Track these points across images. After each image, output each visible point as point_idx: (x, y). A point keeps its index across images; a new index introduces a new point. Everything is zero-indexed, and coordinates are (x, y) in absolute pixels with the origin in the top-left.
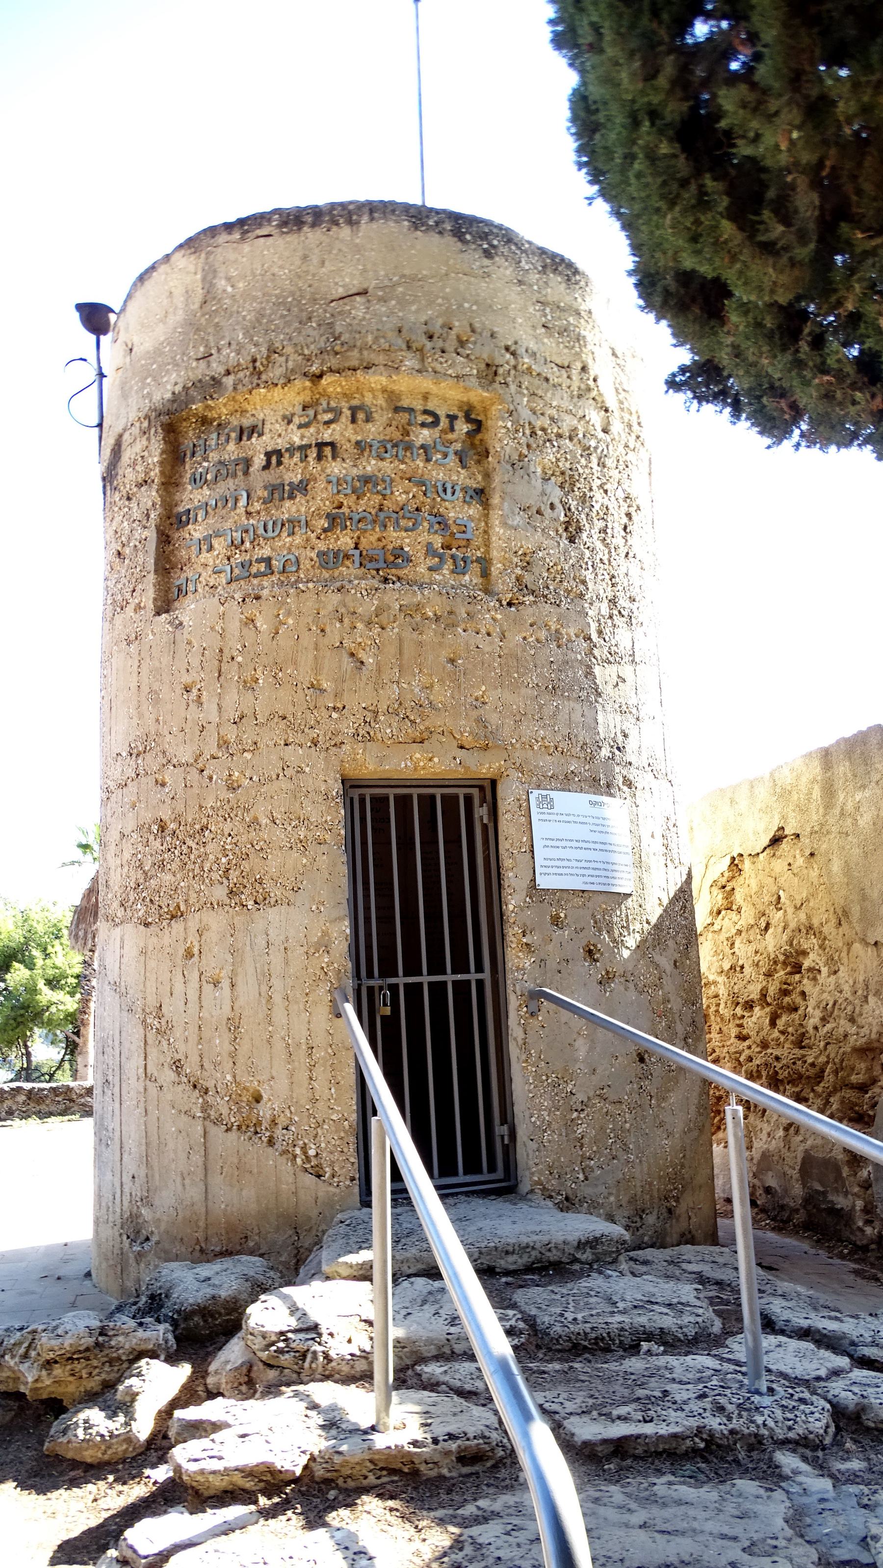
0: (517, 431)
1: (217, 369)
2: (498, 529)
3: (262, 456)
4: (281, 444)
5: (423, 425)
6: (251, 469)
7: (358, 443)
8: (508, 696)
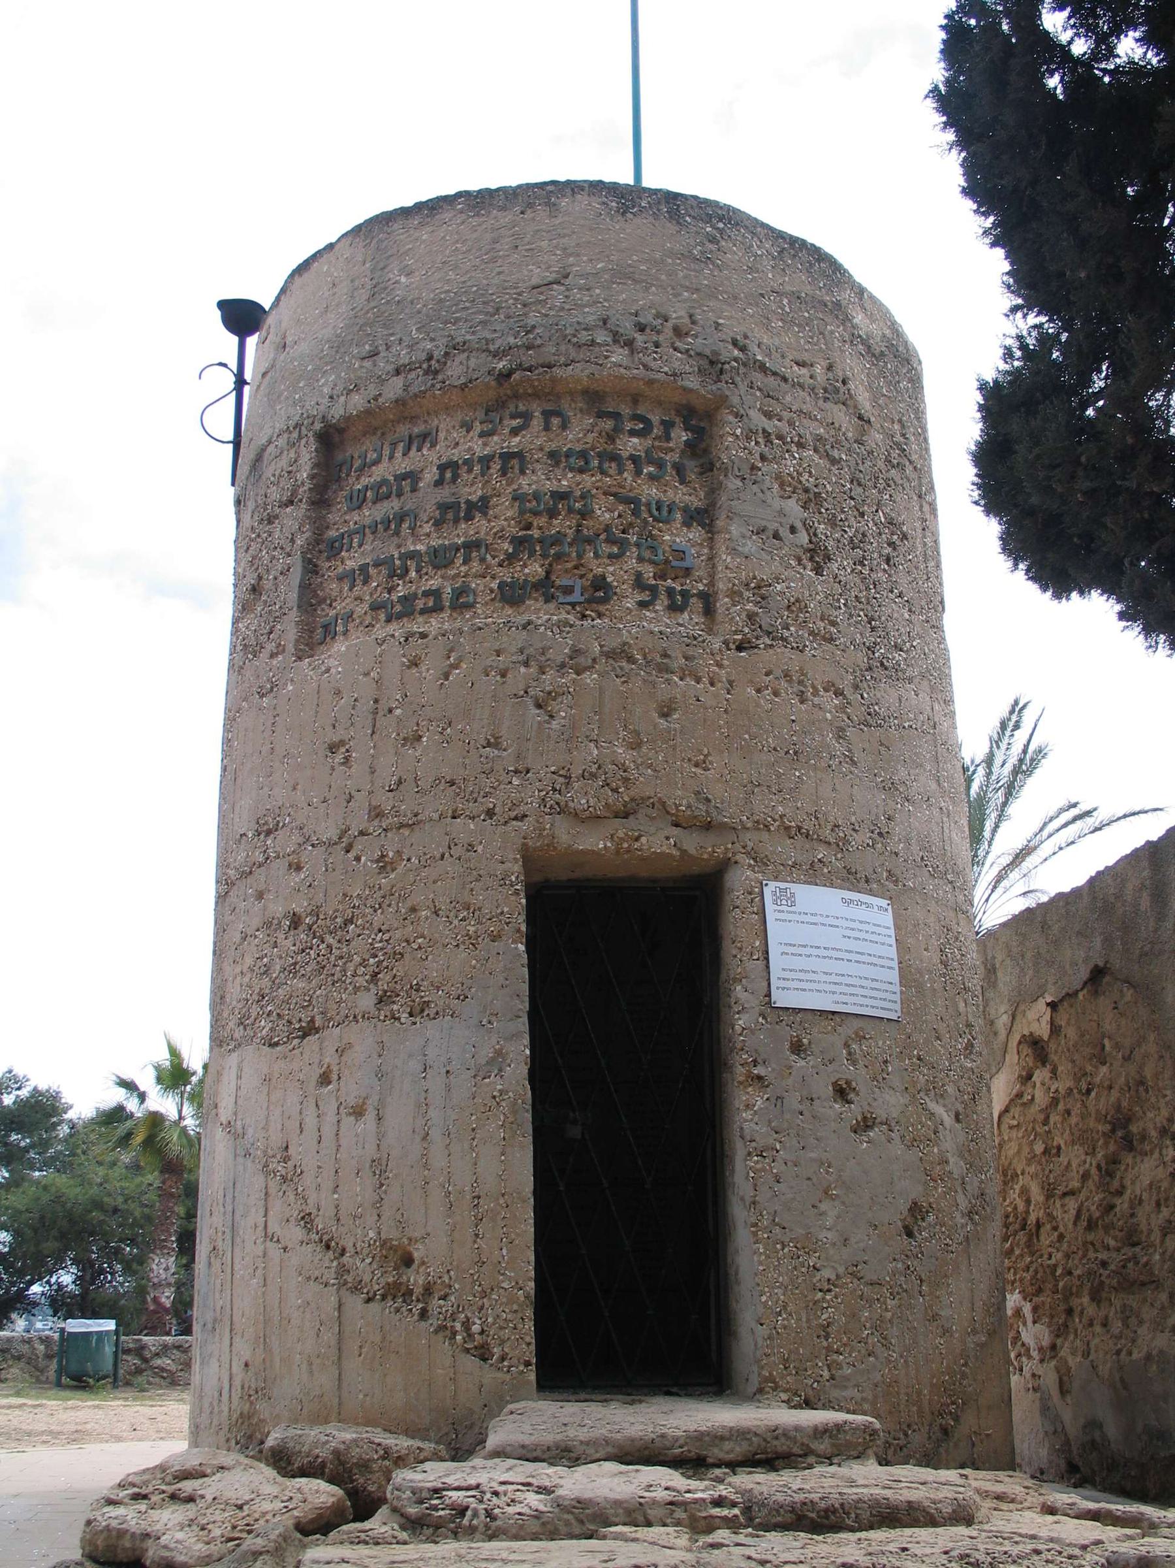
4: (456, 455)
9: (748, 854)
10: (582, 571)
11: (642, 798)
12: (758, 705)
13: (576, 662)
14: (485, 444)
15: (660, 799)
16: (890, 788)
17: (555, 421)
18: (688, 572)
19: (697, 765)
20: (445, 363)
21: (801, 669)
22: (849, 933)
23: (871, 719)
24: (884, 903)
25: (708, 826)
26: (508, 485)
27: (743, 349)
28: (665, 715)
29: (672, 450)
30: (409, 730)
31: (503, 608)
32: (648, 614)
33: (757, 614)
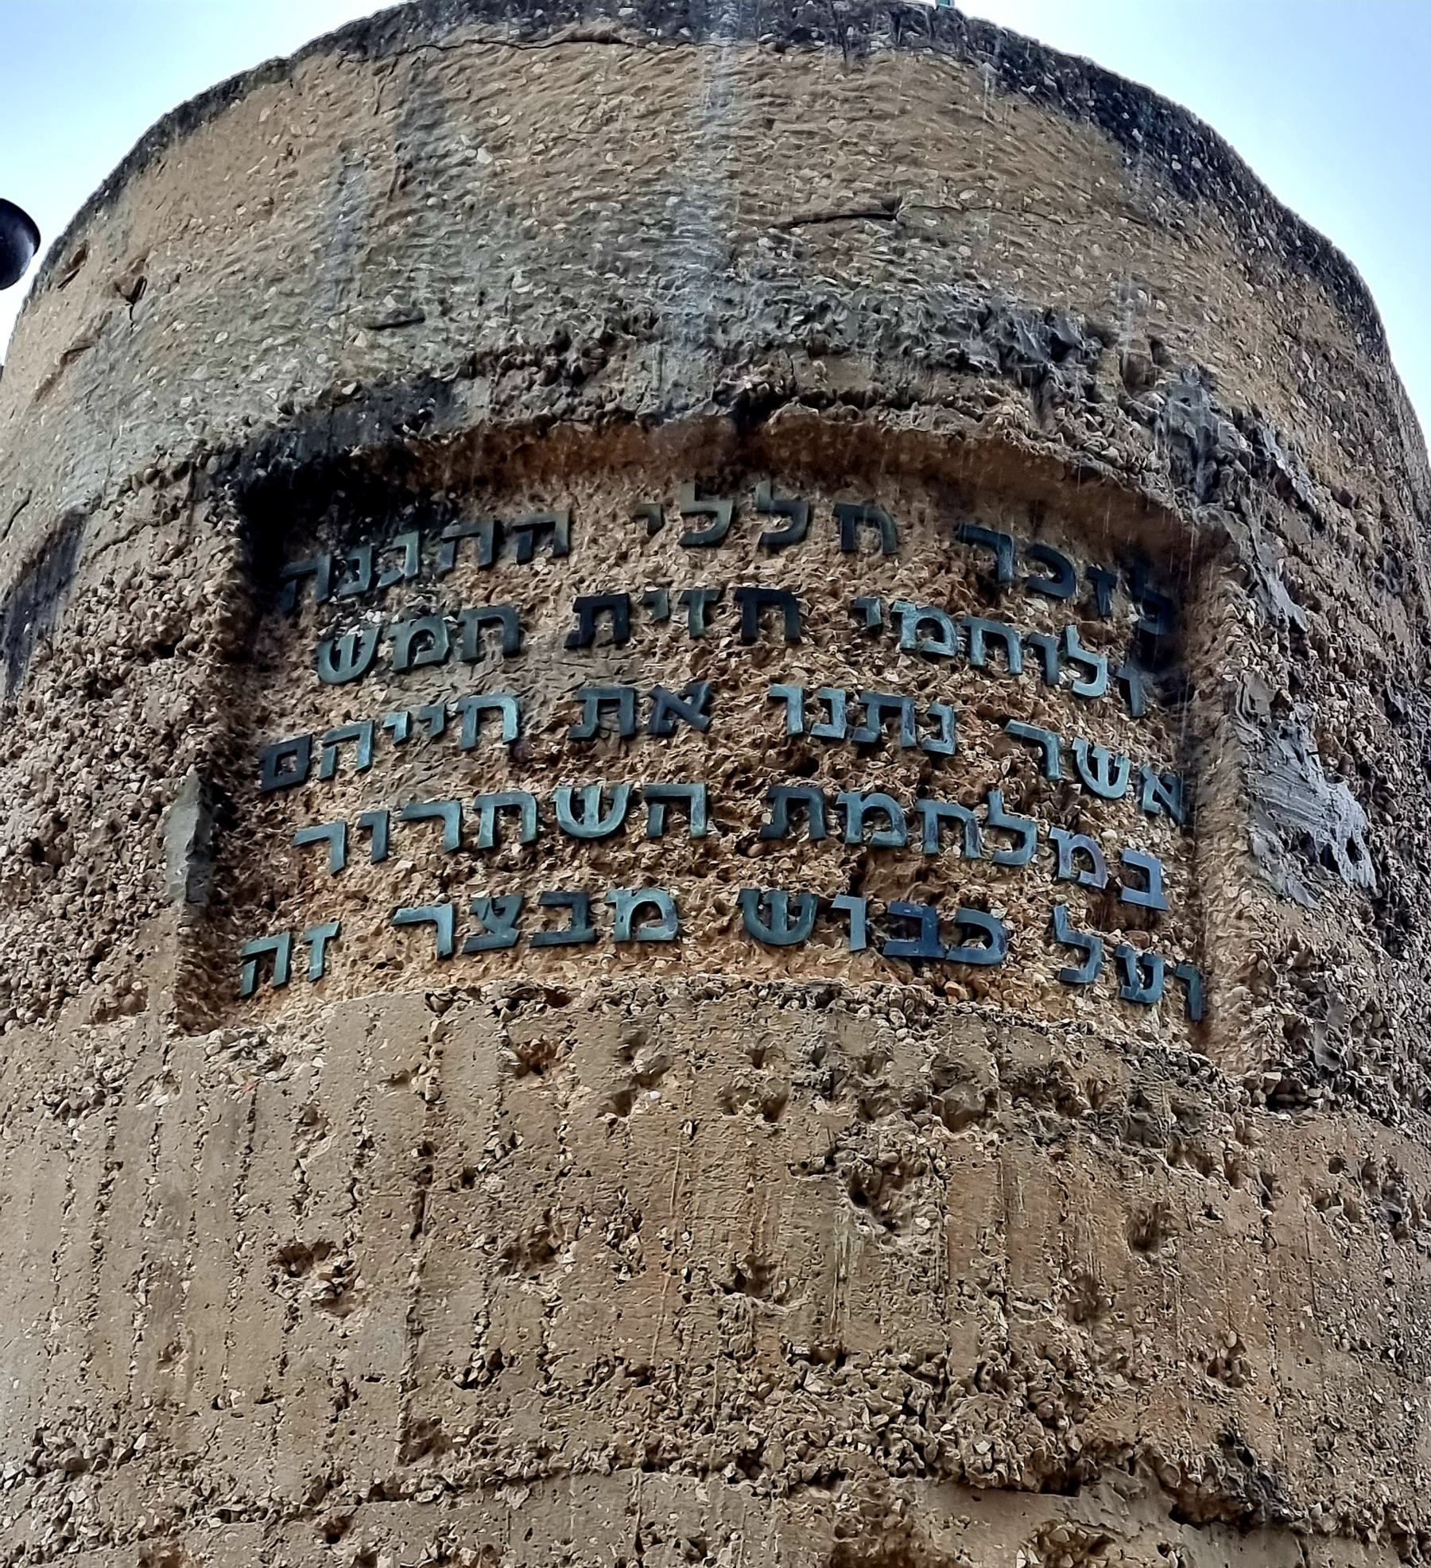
1: (431, 351)
2: (1229, 893)
3: (568, 610)
4: (625, 580)
5: (1033, 589)
6: (531, 640)
7: (858, 611)
10: (933, 886)
11: (1109, 1445)
14: (696, 566)
15: (1148, 1450)
18: (1151, 919)
19: (1213, 1371)
20: (604, 362)
21: (1391, 1165)
26: (760, 665)
27: (1254, 437)
28: (1143, 1245)
31: (749, 953)
32: (1080, 1002)
33: (1306, 1028)
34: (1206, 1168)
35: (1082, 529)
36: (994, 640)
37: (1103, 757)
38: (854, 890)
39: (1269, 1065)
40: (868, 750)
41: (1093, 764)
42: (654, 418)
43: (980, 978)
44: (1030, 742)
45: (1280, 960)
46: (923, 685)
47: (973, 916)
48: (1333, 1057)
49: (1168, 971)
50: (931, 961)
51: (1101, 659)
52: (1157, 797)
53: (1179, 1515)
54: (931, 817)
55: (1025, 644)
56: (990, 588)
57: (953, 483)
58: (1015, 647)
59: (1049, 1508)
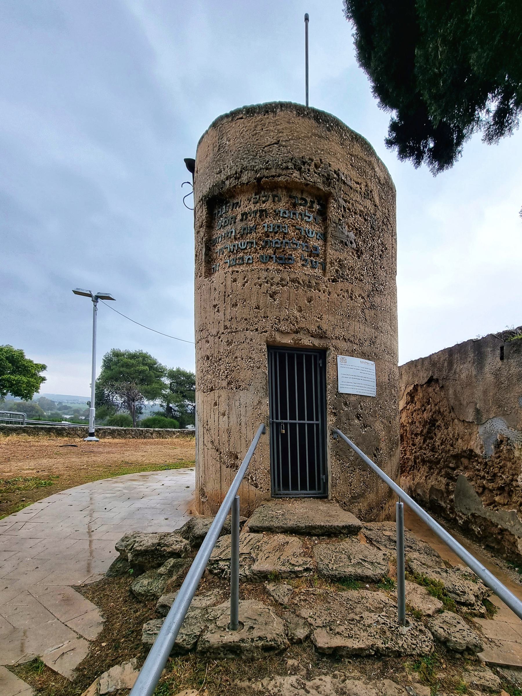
0: (338, 209)
8: (331, 318)
9: (333, 346)
12: (338, 300)
13: (282, 283)
16: (376, 328)
17: (276, 199)
19: (318, 318)
21: (352, 290)
22: (362, 371)
23: (372, 307)
24: (373, 363)
25: (321, 338)
26: (262, 221)
28: (309, 302)
29: (314, 212)
30: (233, 303)
34: (320, 291)
35: (310, 194)
36: (294, 214)
37: (311, 231)
38: (274, 254)
39: (332, 276)
40: (276, 233)
41: (309, 232)
42: (247, 184)
43: (290, 266)
44: (299, 229)
45: (336, 260)
46: (283, 222)
47: (290, 257)
48: (343, 274)
49: (319, 263)
50: (284, 264)
51: (311, 216)
52: (319, 236)
53: (312, 336)
54: (284, 242)
55: (299, 214)
56: (294, 205)
57: (290, 188)
58: (297, 215)
59: (294, 335)
